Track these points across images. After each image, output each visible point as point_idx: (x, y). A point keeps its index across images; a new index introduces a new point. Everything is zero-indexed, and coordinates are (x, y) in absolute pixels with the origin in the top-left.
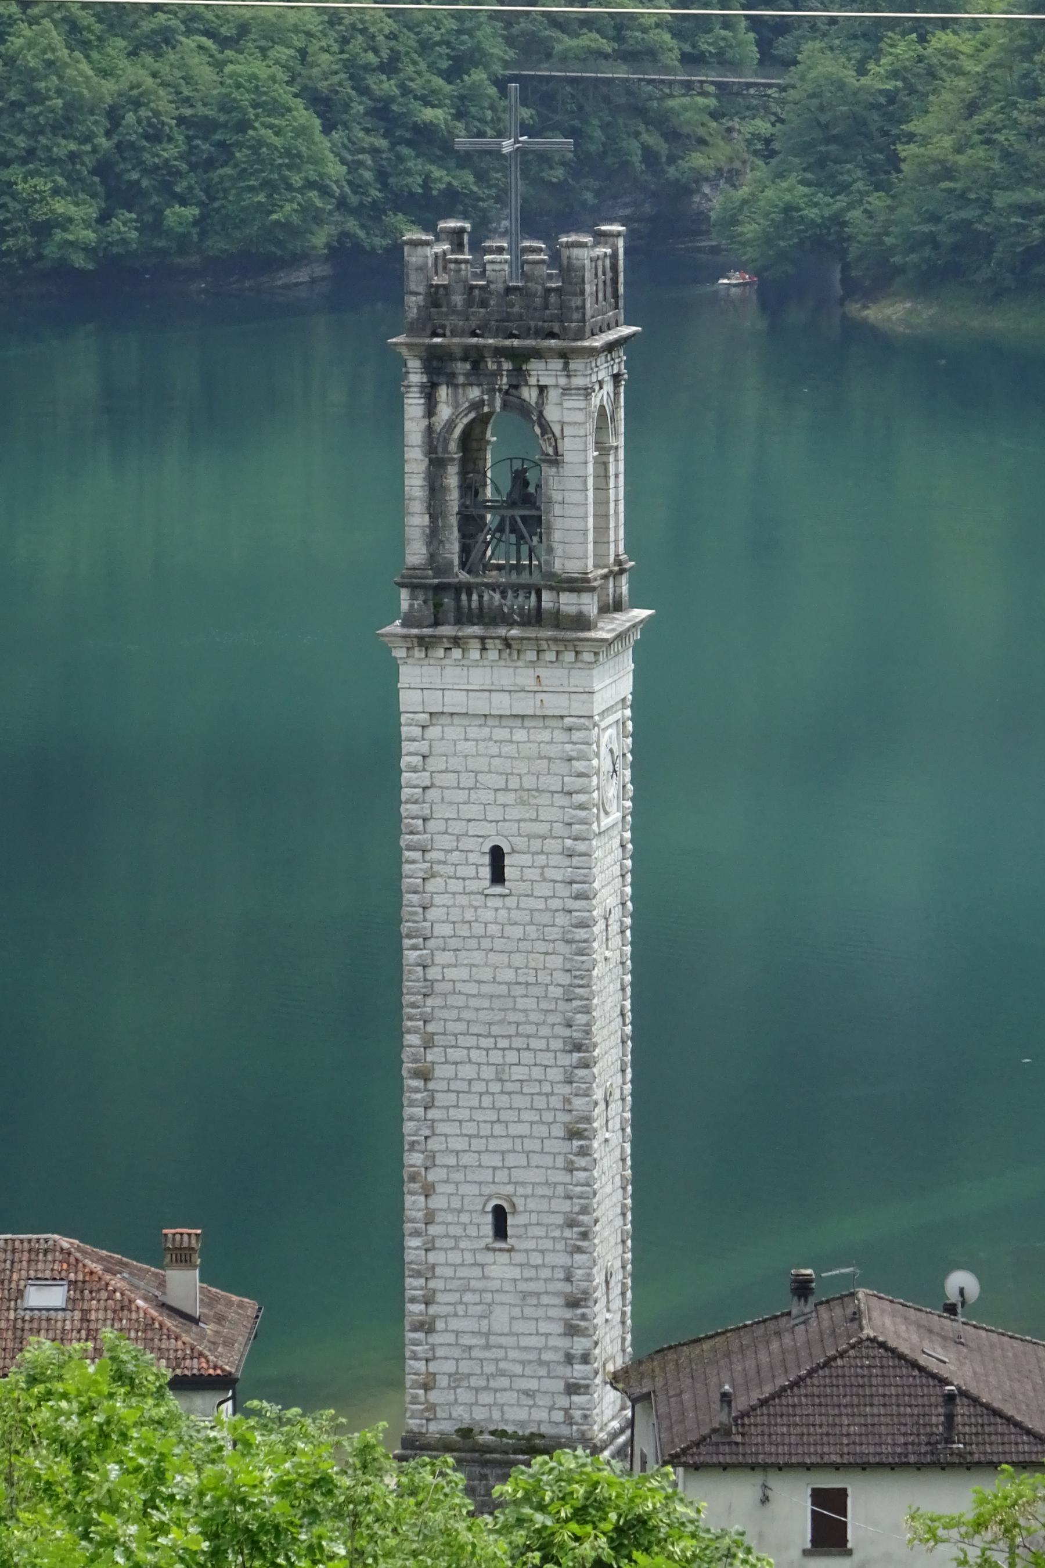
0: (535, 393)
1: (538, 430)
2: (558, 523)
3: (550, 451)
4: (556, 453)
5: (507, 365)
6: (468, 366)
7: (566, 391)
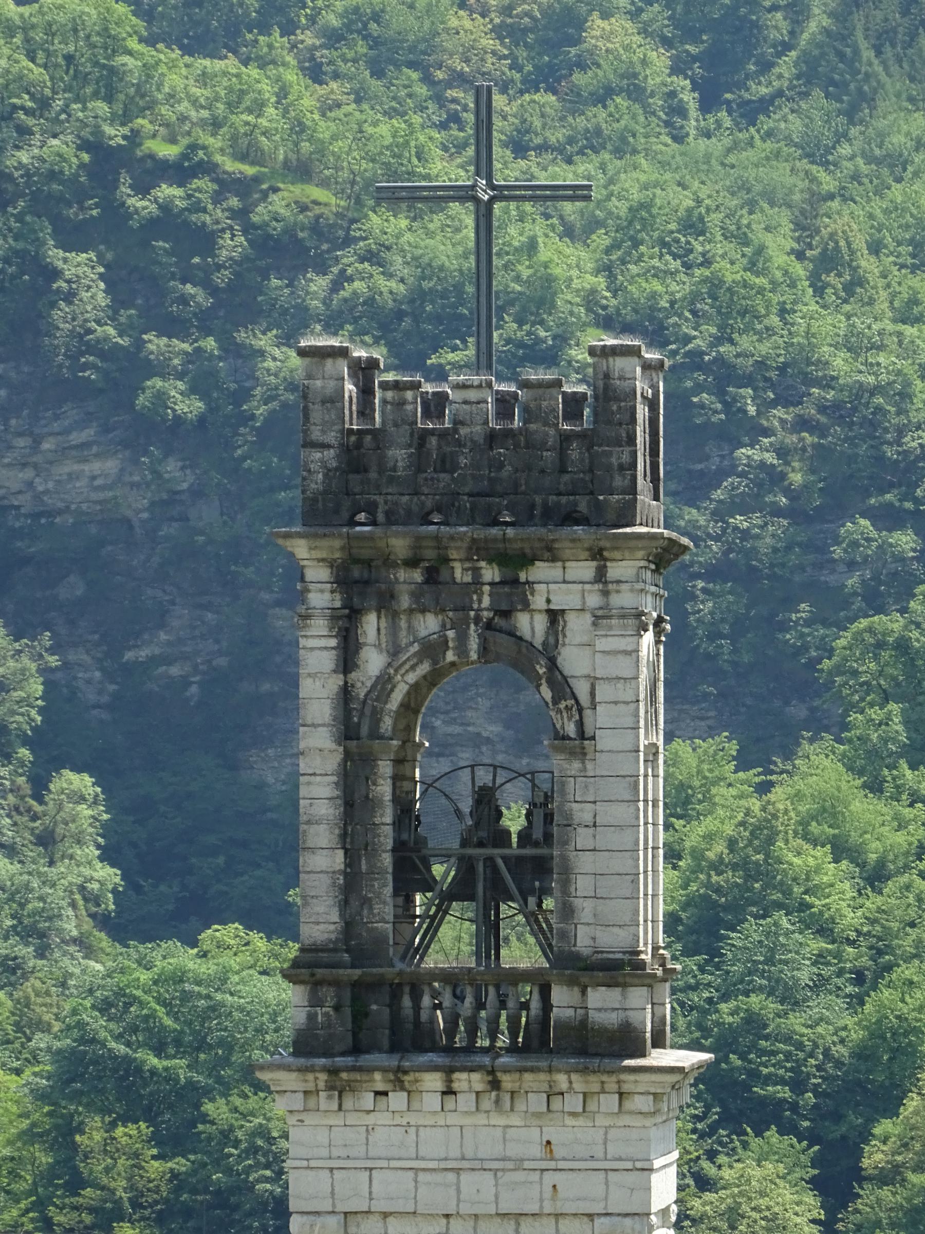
0: (541, 623)
1: (546, 693)
2: (584, 863)
3: (571, 729)
4: (582, 734)
5: (490, 573)
6: (417, 576)
7: (600, 617)
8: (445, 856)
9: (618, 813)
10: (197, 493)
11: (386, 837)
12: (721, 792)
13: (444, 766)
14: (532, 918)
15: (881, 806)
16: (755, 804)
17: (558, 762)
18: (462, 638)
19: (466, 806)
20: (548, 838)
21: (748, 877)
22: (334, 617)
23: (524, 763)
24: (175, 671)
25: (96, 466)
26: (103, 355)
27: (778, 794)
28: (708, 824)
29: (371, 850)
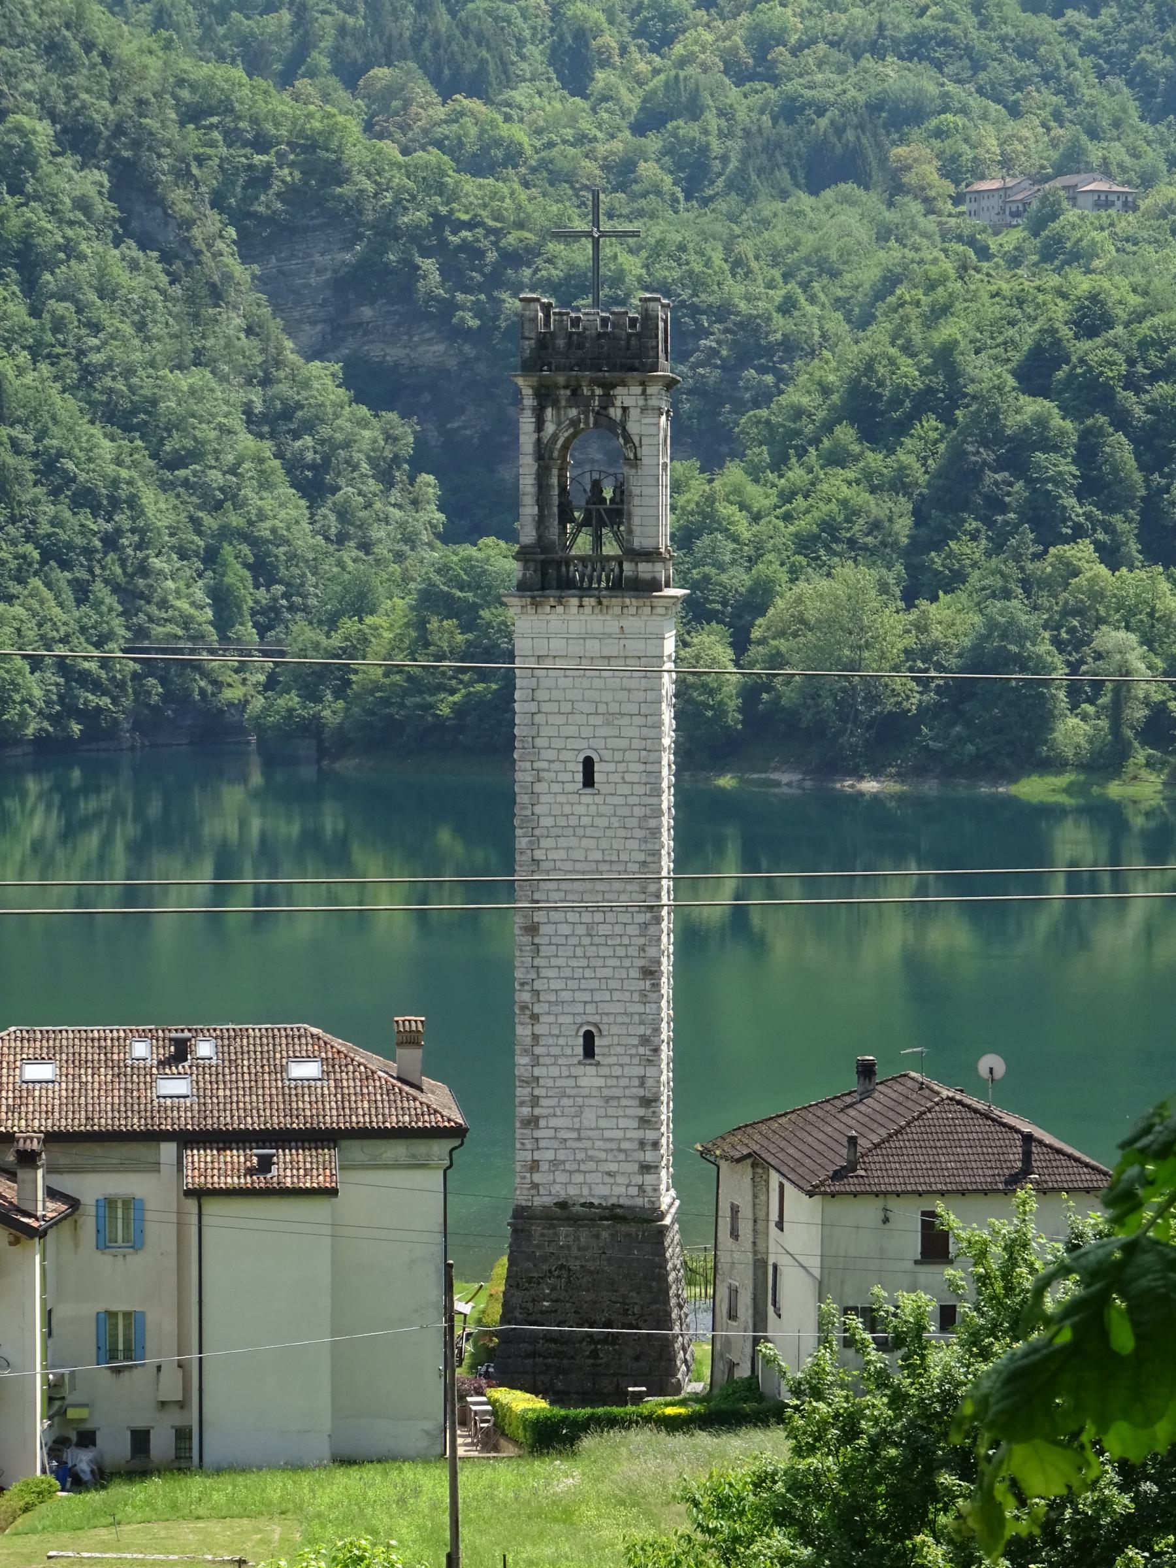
0: (619, 412)
1: (621, 441)
2: (637, 511)
3: (632, 456)
4: (636, 458)
5: (598, 391)
6: (568, 392)
7: (644, 409)
8: (579, 509)
9: (651, 491)
10: (477, 359)
11: (555, 501)
12: (693, 483)
13: (579, 471)
14: (615, 534)
15: (758, 488)
16: (707, 488)
17: (626, 470)
18: (587, 418)
19: (588, 488)
20: (622, 501)
21: (704, 518)
22: (534, 409)
23: (612, 471)
24: (468, 432)
25: (435, 348)
26: (438, 301)
27: (716, 484)
28: (687, 496)
29: (549, 506)
